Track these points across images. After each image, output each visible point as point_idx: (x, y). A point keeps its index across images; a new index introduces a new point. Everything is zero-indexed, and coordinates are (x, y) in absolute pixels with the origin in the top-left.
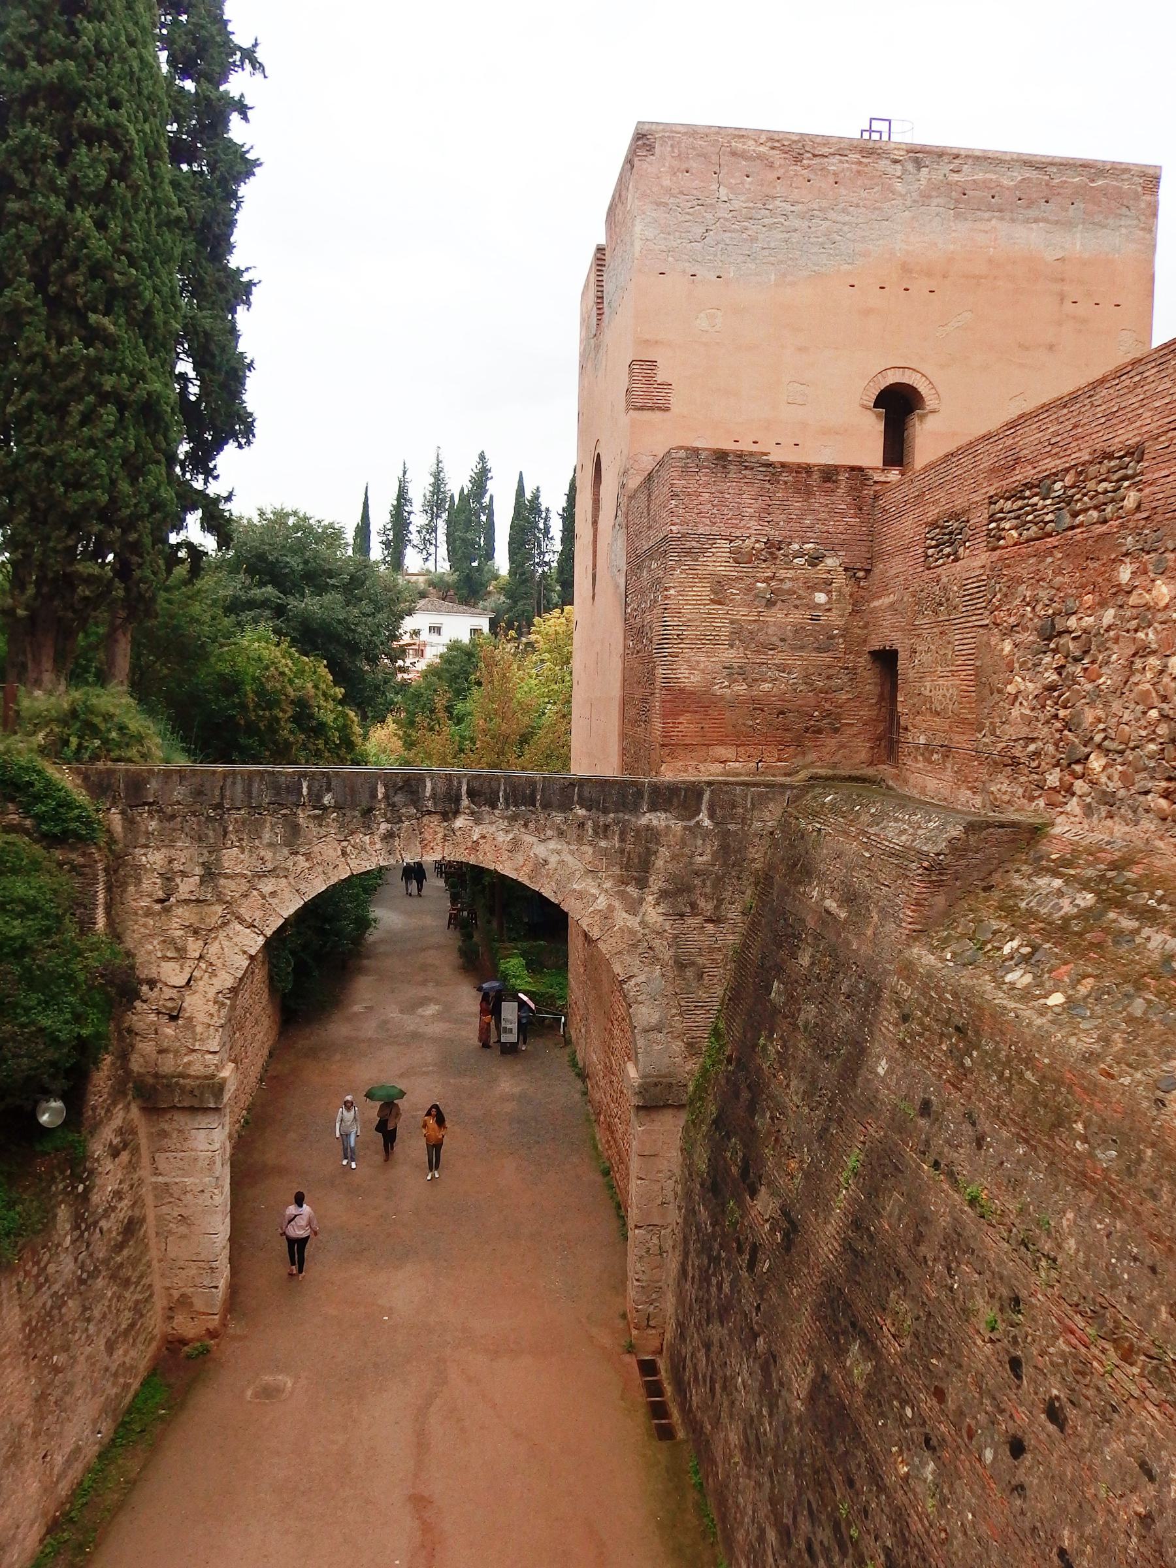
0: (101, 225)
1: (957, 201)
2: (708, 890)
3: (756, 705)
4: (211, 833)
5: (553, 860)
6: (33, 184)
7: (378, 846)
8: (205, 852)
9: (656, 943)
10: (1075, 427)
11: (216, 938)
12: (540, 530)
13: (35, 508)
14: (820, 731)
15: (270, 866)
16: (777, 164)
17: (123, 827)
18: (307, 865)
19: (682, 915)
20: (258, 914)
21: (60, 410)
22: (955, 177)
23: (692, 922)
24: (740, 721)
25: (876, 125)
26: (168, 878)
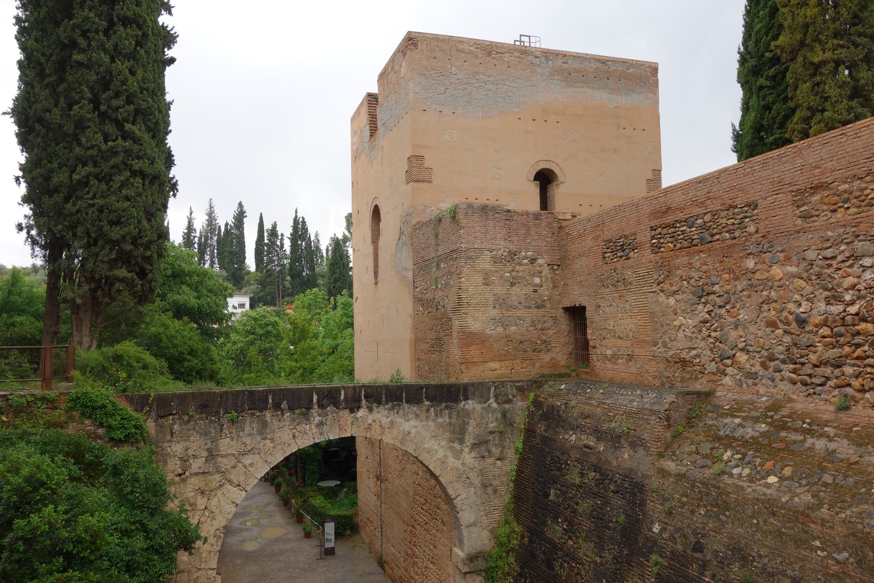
0: (133, 73)
1: (567, 77)
2: (497, 442)
3: (509, 339)
4: (213, 430)
5: (413, 431)
6: (89, 45)
7: (314, 431)
8: (209, 442)
9: (471, 475)
10: (708, 193)
11: (215, 495)
12: (278, 246)
13: (89, 237)
14: (540, 351)
15: (249, 448)
16: (480, 56)
17: (156, 430)
18: (272, 445)
19: (483, 457)
20: (242, 478)
21: (106, 178)
22: (565, 66)
23: (489, 461)
24: (501, 348)
25: (523, 39)
26: (184, 460)
